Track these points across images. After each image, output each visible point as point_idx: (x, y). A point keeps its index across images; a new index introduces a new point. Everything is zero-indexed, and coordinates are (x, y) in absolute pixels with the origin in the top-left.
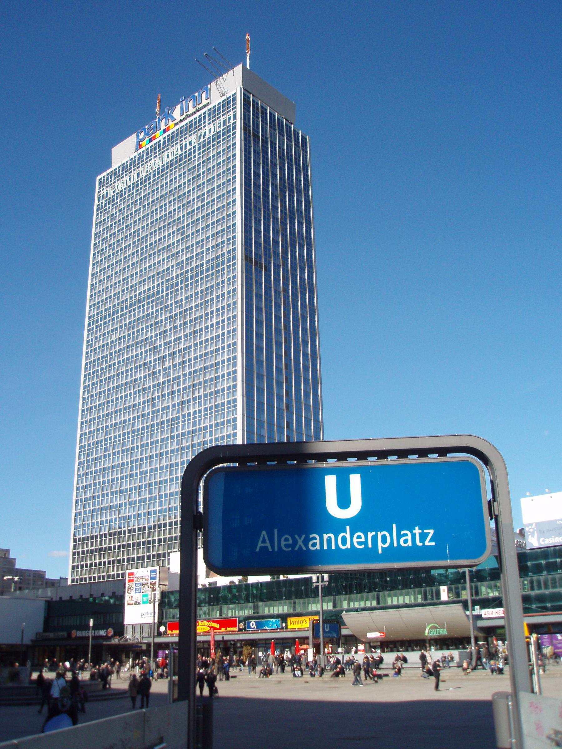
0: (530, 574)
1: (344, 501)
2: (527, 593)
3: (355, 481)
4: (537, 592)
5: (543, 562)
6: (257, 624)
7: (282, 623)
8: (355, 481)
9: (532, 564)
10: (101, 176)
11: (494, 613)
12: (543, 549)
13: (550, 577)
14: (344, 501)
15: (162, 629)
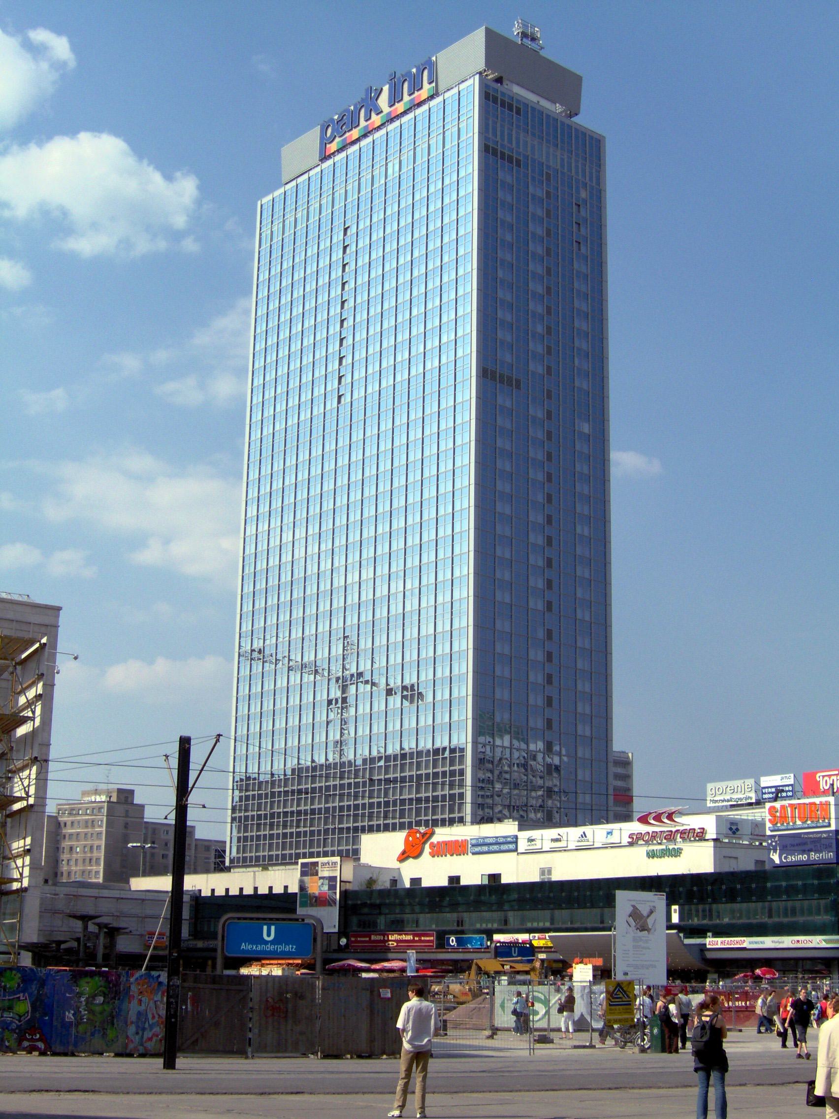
0: (769, 898)
1: (269, 935)
2: (763, 921)
3: (273, 928)
4: (776, 919)
5: (784, 884)
6: (458, 940)
7: (488, 940)
8: (273, 928)
9: (772, 886)
10: (265, 200)
11: (719, 943)
12: (784, 868)
13: (790, 904)
14: (269, 935)
15: (343, 941)
